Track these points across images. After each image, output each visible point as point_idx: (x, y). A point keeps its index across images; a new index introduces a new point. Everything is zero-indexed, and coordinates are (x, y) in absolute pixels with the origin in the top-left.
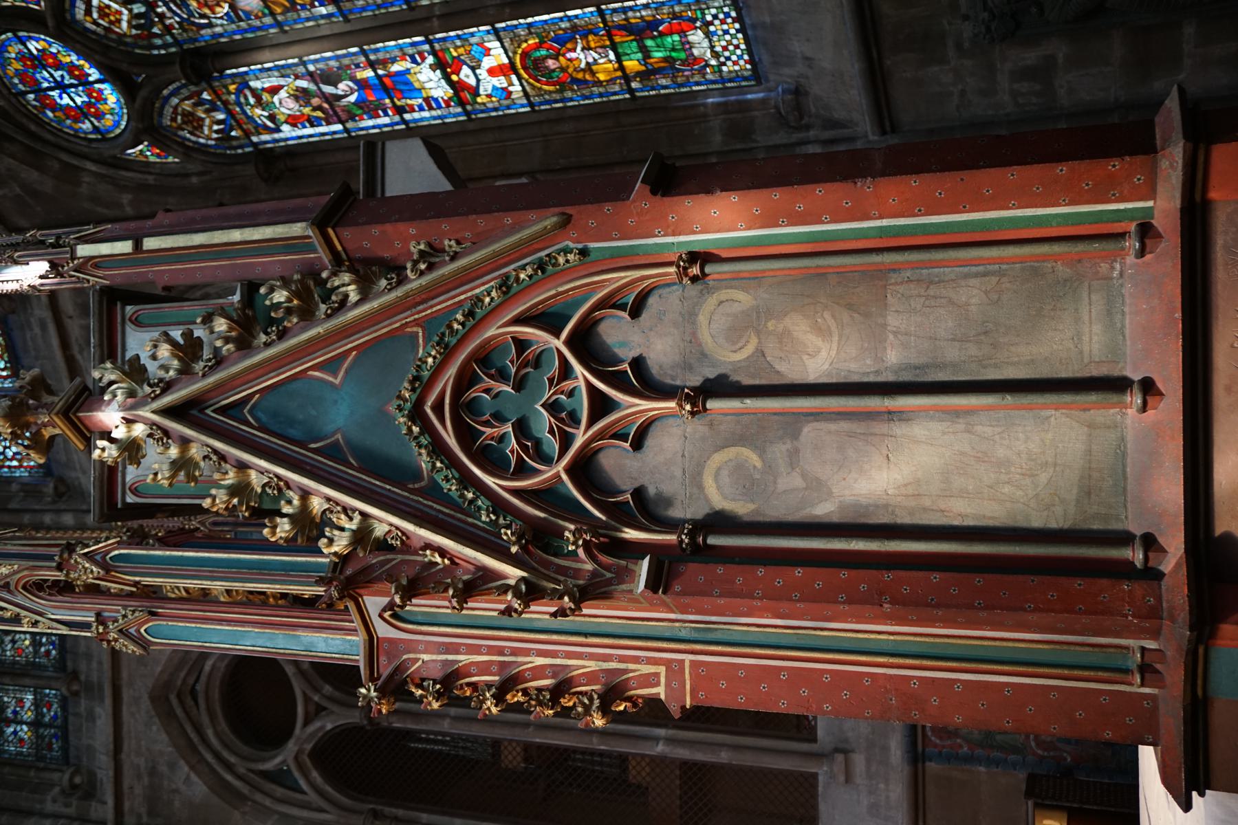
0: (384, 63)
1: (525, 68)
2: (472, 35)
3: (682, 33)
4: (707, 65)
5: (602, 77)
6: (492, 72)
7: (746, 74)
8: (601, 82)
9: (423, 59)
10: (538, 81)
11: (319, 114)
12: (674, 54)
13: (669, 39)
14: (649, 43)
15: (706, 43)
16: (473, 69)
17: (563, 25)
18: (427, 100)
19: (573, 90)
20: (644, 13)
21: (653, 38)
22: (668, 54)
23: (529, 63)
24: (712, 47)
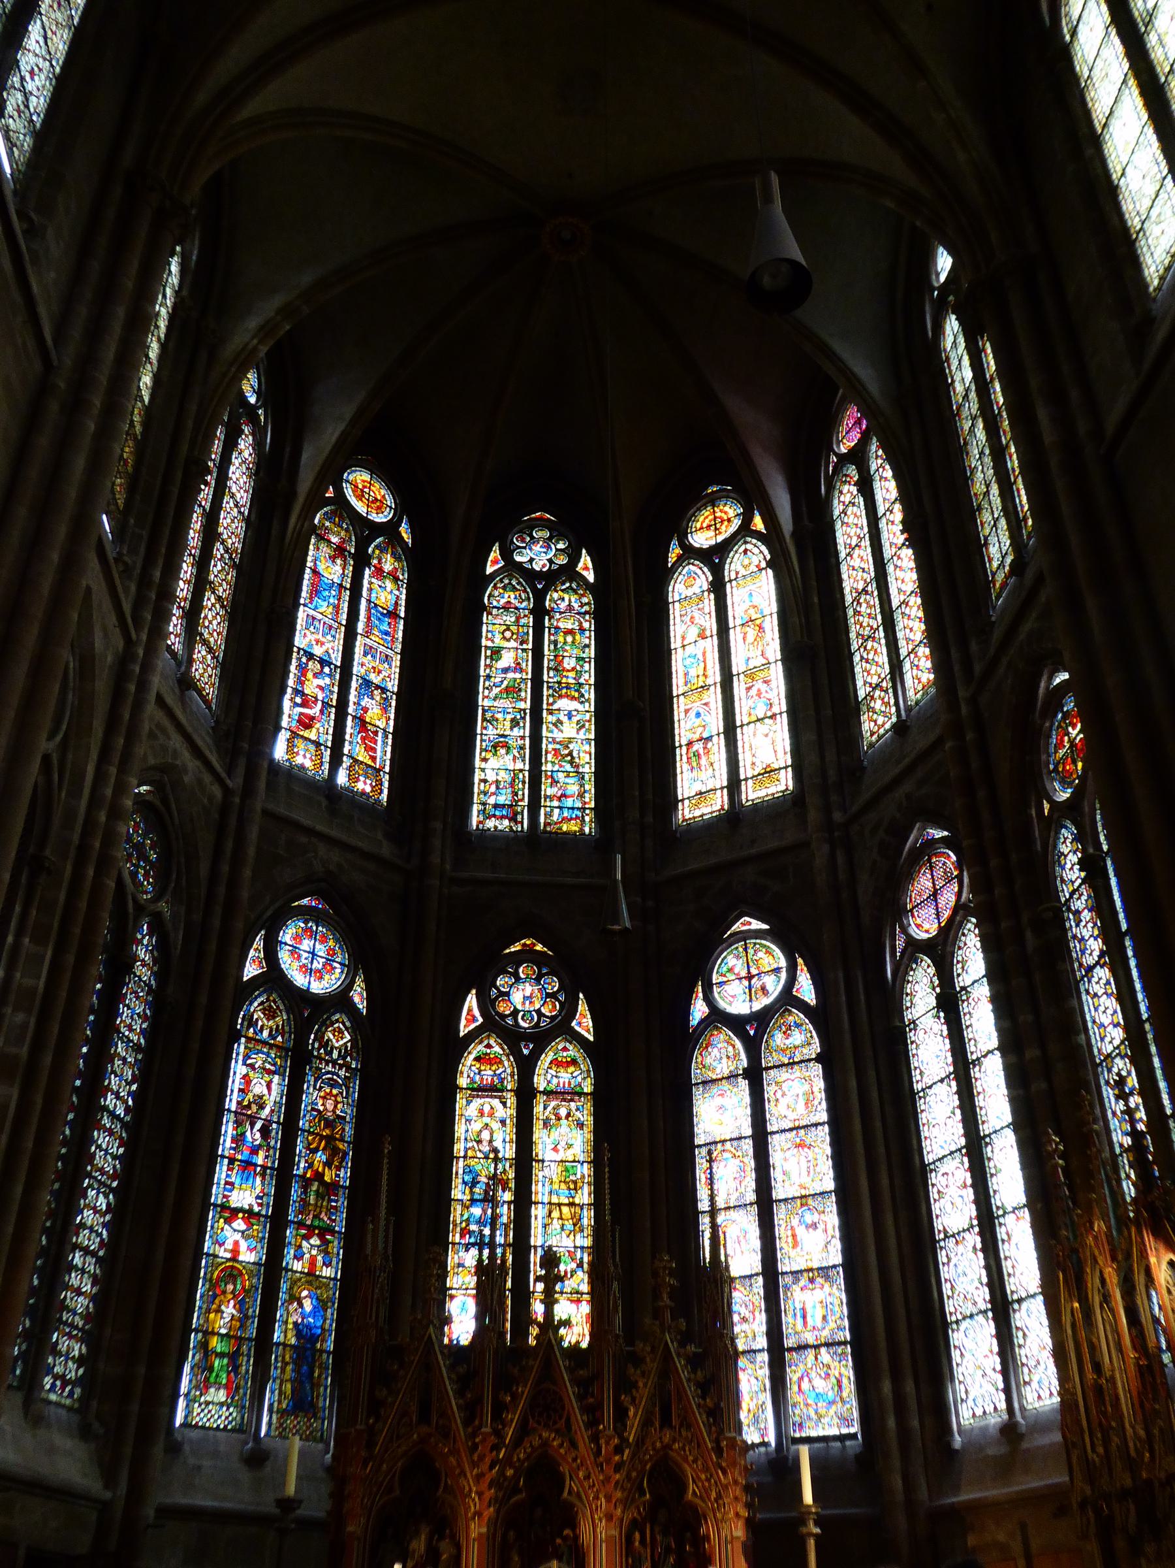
0: (263, 1176)
1: (232, 1267)
2: (262, 1248)
3: (227, 1387)
4: (201, 1395)
5: (212, 1316)
6: (236, 1243)
7: (190, 1419)
8: (209, 1313)
9: (260, 1205)
10: (222, 1271)
11: (246, 1103)
12: (214, 1374)
13: (224, 1376)
14: (225, 1361)
15: (216, 1400)
16: (243, 1232)
17: (251, 1310)
18: (232, 1184)
19: (209, 1290)
20: (244, 1368)
21: (228, 1367)
22: (216, 1369)
23: (235, 1273)
24: (212, 1403)
